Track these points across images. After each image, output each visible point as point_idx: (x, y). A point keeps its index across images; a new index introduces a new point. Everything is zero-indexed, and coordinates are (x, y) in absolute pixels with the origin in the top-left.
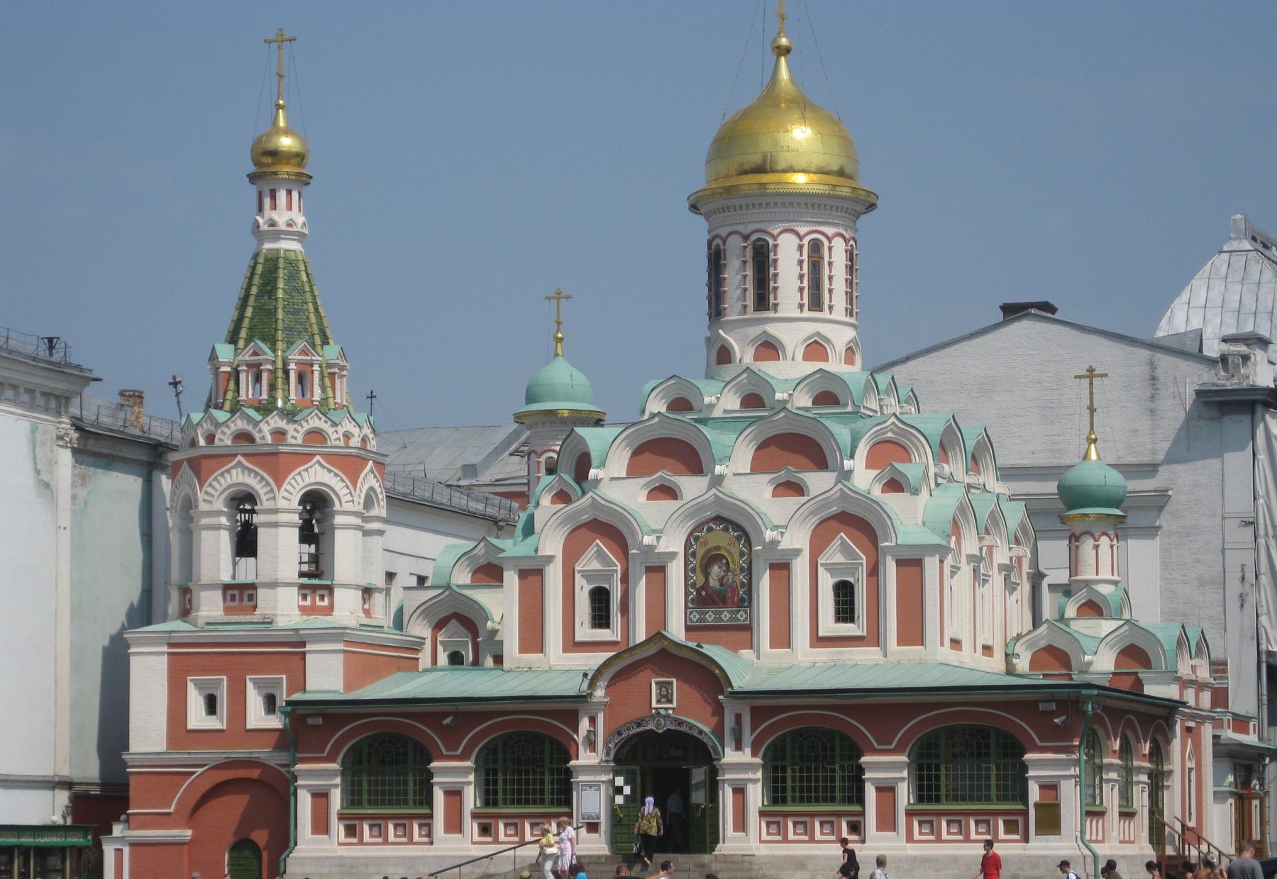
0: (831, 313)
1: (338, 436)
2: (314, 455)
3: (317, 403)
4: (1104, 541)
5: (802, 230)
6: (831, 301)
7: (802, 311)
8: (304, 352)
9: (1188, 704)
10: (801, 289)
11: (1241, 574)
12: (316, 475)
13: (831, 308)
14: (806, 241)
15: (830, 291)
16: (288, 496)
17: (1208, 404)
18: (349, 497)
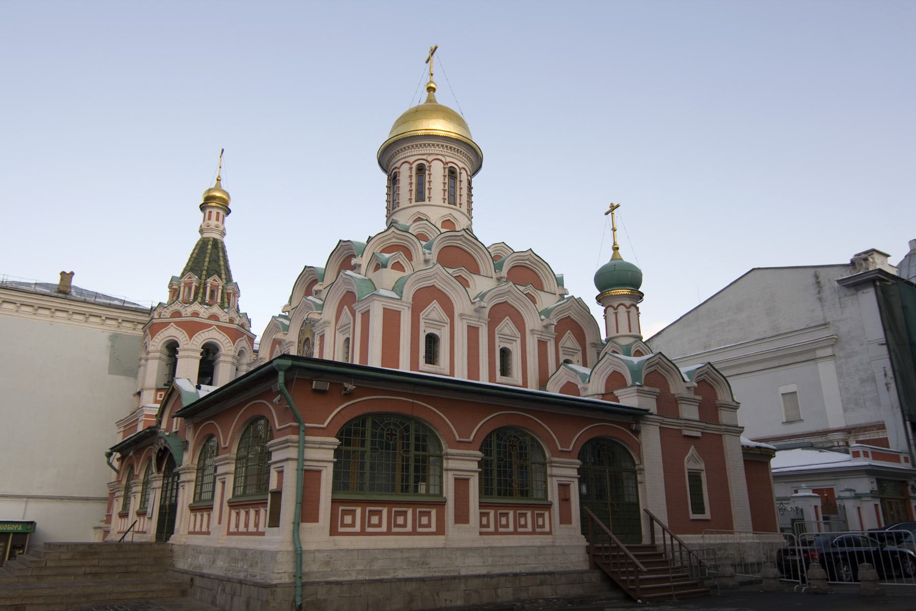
0: (430, 201)
1: (186, 313)
2: (171, 322)
3: (191, 300)
4: (622, 309)
5: (411, 159)
6: (430, 194)
7: (411, 203)
8: (190, 278)
9: (650, 412)
10: (411, 191)
11: (884, 373)
12: (173, 332)
13: (430, 198)
14: (414, 166)
15: (430, 189)
16: (154, 343)
17: (848, 287)
18: (186, 342)
